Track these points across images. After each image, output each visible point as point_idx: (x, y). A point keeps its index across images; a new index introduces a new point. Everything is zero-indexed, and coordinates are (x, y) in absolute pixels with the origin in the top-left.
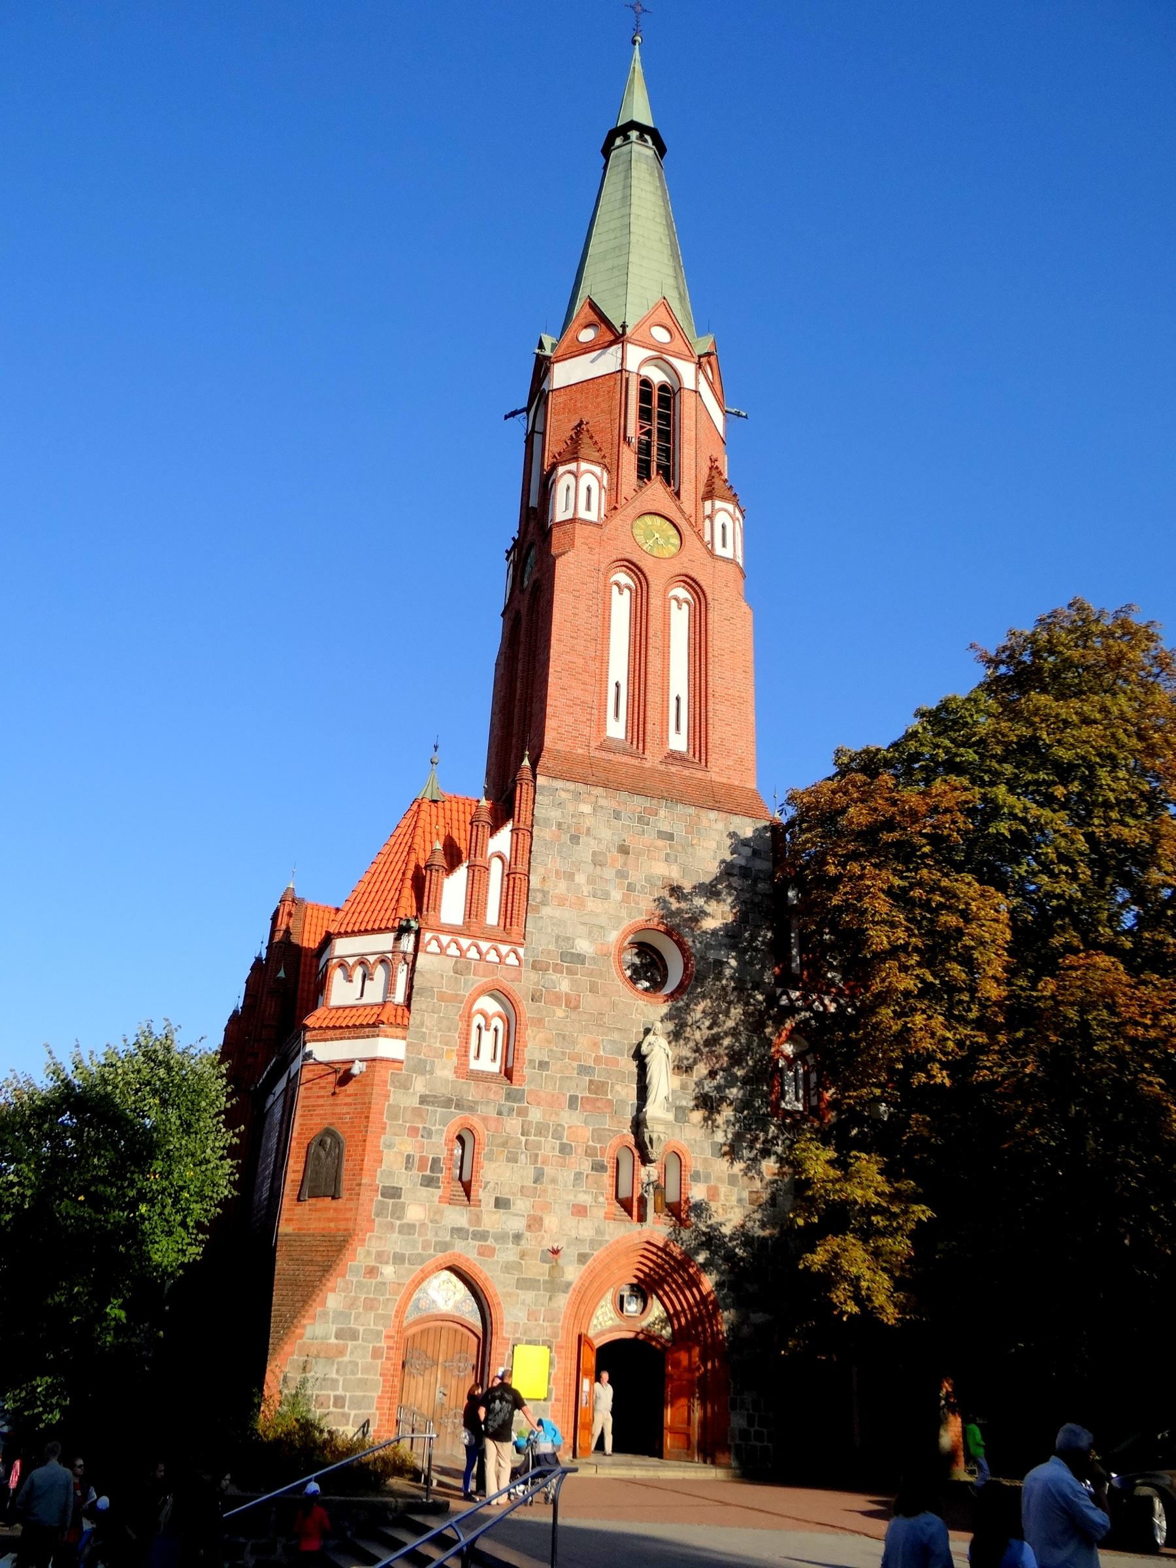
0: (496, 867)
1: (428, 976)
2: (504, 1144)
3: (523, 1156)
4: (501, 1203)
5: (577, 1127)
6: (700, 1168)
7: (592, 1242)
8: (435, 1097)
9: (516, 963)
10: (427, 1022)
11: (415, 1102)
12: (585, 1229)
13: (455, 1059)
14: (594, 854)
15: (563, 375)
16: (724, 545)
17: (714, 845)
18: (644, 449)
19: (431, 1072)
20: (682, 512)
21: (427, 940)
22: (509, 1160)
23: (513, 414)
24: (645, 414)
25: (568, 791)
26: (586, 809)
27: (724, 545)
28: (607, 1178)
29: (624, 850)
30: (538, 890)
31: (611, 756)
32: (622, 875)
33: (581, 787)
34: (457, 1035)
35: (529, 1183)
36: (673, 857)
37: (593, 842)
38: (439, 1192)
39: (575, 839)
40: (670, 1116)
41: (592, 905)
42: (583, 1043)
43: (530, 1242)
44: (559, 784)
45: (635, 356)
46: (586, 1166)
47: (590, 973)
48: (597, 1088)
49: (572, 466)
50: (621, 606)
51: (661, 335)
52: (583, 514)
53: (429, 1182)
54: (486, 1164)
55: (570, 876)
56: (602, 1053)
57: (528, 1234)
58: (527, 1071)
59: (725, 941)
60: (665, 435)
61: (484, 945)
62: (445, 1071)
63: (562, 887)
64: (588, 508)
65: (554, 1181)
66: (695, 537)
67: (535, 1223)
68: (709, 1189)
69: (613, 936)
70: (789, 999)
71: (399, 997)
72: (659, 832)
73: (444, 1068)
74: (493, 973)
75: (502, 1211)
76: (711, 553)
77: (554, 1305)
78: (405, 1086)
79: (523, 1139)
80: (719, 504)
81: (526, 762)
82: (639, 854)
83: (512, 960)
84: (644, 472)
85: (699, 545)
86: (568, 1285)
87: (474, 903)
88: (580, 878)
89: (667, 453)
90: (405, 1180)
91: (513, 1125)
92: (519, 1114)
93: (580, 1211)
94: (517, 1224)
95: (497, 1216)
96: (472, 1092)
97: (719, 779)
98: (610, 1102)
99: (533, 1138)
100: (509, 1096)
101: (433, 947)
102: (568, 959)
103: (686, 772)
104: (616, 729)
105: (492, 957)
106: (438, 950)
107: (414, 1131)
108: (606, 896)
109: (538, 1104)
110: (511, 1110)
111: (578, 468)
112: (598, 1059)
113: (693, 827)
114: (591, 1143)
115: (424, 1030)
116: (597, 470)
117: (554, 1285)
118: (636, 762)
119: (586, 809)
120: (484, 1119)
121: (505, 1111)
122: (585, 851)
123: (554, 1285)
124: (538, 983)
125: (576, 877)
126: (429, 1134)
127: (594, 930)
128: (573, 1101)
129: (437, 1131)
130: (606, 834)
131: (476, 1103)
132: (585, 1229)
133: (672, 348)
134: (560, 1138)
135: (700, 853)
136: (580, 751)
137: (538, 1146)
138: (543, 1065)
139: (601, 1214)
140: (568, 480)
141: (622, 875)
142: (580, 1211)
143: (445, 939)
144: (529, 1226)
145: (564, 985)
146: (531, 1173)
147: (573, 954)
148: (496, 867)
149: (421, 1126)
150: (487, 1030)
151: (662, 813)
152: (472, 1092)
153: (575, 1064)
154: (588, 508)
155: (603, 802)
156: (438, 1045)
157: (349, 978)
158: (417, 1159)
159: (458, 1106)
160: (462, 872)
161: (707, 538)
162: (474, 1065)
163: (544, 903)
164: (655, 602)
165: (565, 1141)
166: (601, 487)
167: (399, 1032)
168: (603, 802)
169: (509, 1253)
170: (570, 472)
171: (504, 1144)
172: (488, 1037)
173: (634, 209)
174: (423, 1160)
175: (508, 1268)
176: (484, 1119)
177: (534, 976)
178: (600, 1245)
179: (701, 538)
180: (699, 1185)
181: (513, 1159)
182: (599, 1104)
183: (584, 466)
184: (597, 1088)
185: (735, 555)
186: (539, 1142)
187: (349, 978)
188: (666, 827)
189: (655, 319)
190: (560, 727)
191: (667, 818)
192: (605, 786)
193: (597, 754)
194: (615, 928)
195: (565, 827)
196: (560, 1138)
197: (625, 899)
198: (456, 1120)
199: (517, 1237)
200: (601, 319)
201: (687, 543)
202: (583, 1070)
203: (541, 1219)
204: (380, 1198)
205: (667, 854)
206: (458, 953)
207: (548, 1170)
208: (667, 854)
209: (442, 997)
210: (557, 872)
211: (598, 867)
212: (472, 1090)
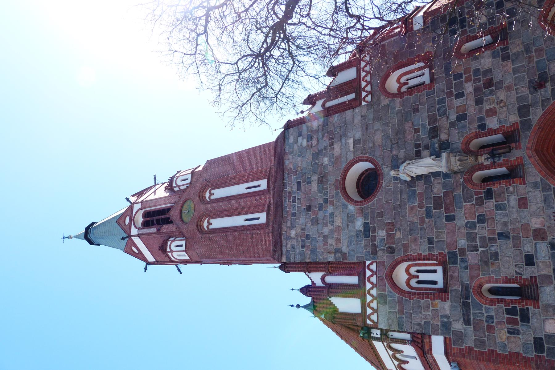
0: (330, 279)
1: (390, 321)
3: (492, 248)
4: (530, 260)
5: (465, 213)
6: (476, 125)
7: (544, 190)
8: (463, 314)
9: (375, 264)
10: (418, 321)
11: (470, 329)
13: (437, 301)
14: (313, 225)
17: (299, 159)
19: (448, 317)
20: (178, 201)
21: (371, 323)
22: (497, 259)
23: (179, 270)
25: (287, 244)
26: (293, 233)
28: (496, 188)
30: (335, 255)
32: (321, 208)
33: (284, 235)
34: (422, 301)
35: (510, 243)
36: (308, 180)
38: (531, 308)
39: (308, 237)
40: (444, 155)
41: (338, 223)
42: (413, 218)
44: (284, 249)
46: (490, 204)
47: (373, 218)
50: (218, 223)
52: (183, 248)
53: (525, 318)
55: (326, 237)
56: (416, 204)
58: (436, 252)
59: (343, 141)
62: (445, 307)
63: (331, 242)
65: (505, 224)
67: (539, 235)
68: (488, 116)
69: (351, 208)
72: (298, 190)
73: (444, 309)
74: (382, 279)
75: (535, 260)
76: (190, 184)
78: (460, 336)
79: (480, 249)
80: (174, 185)
82: (309, 199)
84: (168, 221)
85: (188, 192)
88: (326, 231)
90: (527, 336)
91: (472, 258)
92: (465, 255)
93: (523, 203)
95: (540, 264)
97: (273, 162)
98: (446, 194)
99: (478, 243)
100: (455, 263)
102: (367, 233)
106: (375, 315)
107: (490, 328)
108: (332, 215)
109: (455, 242)
111: (169, 252)
112: (421, 206)
114: (474, 202)
115: (423, 323)
116: (169, 243)
122: (312, 230)
124: (383, 251)
125: (325, 234)
126: (490, 317)
127: (351, 219)
128: (450, 218)
129: (487, 312)
131: (463, 285)
132: (536, 197)
134: (473, 226)
136: (271, 238)
137: (483, 239)
138: (430, 241)
139: (521, 187)
142: (523, 203)
143: (369, 311)
144: (543, 239)
145: (382, 233)
147: (364, 230)
148: (330, 279)
149: (486, 324)
150: (418, 277)
151: (289, 190)
153: (426, 220)
155: (289, 224)
156: (430, 313)
158: (510, 326)
159: (467, 298)
162: (440, 285)
164: (210, 207)
165: (476, 220)
166: (175, 240)
167: (426, 340)
172: (423, 277)
174: (509, 321)
176: (472, 278)
177: (380, 253)
178: (546, 184)
180: (487, 123)
181: (496, 255)
182: (448, 201)
183: (168, 250)
184: (437, 203)
186: (480, 238)
188: (295, 187)
189: (123, 224)
191: (292, 188)
193: (271, 228)
194: (347, 207)
197: (332, 203)
202: (429, 214)
203: (535, 230)
204: (545, 354)
207: (499, 229)
208: (308, 183)
210: (324, 245)
211: (319, 222)
212: (455, 288)
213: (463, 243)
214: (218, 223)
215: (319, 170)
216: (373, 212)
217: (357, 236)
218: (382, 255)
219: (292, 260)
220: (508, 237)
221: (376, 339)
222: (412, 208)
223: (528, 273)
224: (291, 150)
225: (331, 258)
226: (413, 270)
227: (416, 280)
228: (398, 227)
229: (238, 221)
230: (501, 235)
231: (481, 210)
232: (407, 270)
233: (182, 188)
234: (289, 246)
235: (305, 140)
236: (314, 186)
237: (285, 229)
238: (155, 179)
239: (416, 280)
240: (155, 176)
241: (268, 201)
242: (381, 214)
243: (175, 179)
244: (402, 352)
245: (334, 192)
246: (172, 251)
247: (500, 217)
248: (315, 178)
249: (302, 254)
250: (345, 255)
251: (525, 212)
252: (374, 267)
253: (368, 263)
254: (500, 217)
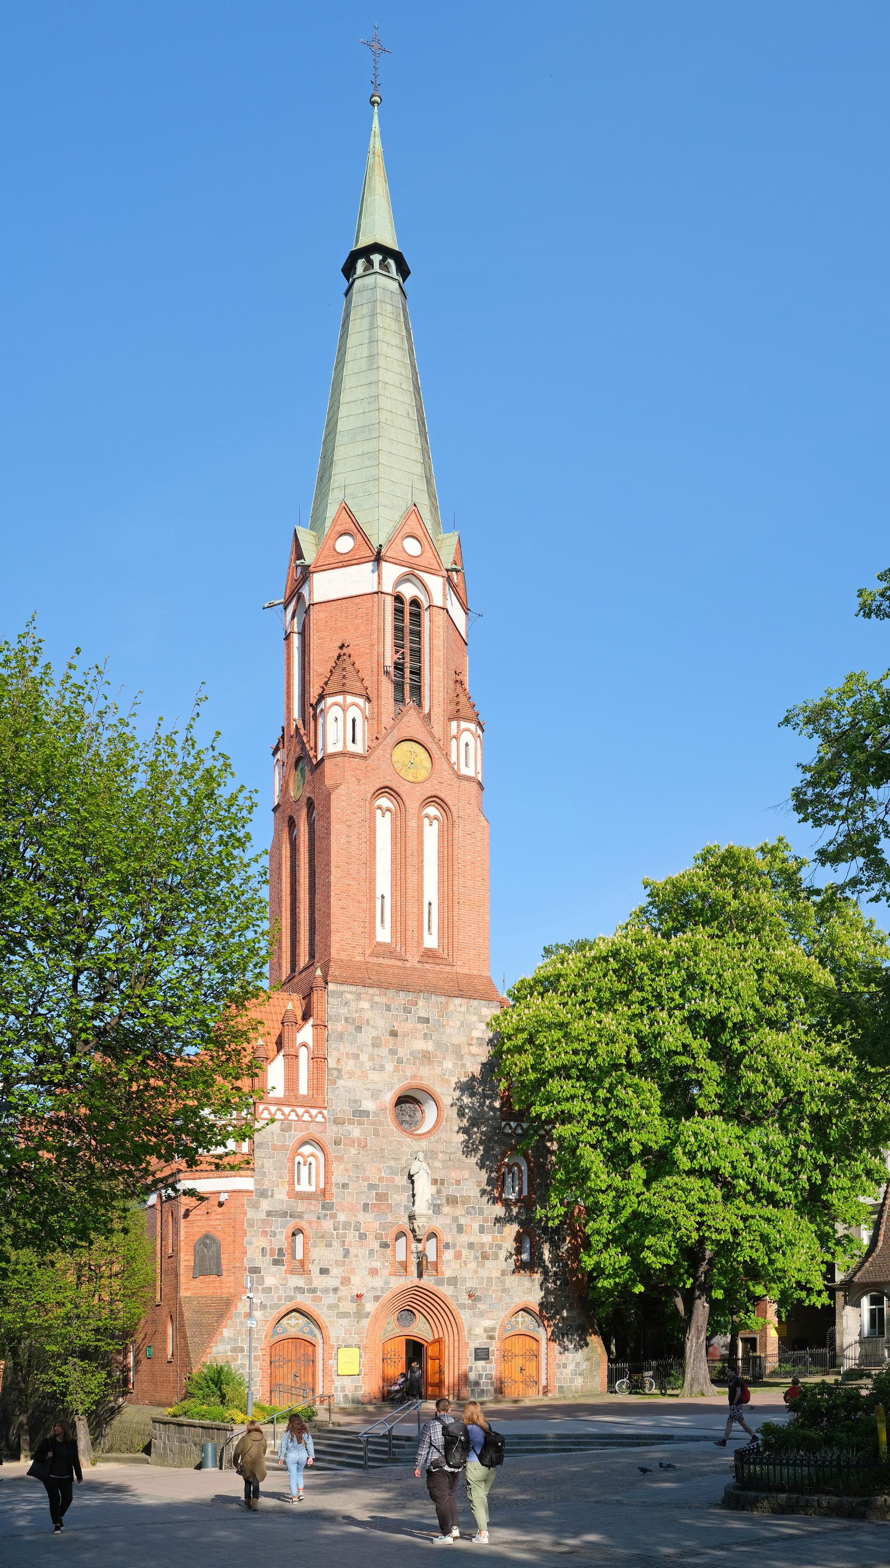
2: (322, 1237)
4: (324, 1271)
12: (378, 1282)
15: (325, 586)
17: (458, 1023)
22: (326, 1246)
25: (351, 993)
26: (365, 1005)
29: (394, 1034)
31: (381, 960)
32: (393, 1052)
33: (360, 989)
35: (341, 1258)
37: (371, 1030)
39: (359, 1029)
43: (343, 1291)
45: (391, 572)
46: (376, 1245)
48: (382, 1197)
50: (384, 826)
51: (412, 547)
54: (312, 1249)
55: (356, 1057)
57: (342, 1288)
58: (334, 1190)
60: (417, 654)
61: (301, 1111)
63: (350, 1065)
65: (356, 1256)
66: (444, 760)
67: (346, 1281)
69: (389, 1097)
70: (522, 1129)
77: (360, 1325)
81: (319, 972)
82: (405, 1035)
83: (320, 1119)
84: (399, 699)
86: (369, 1314)
87: (291, 1081)
88: (364, 1058)
93: (373, 1272)
94: (336, 1283)
96: (301, 1206)
100: (323, 1207)
103: (438, 968)
104: (383, 935)
105: (306, 1117)
108: (382, 1068)
110: (326, 1215)
112: (381, 1179)
113: (443, 1011)
117: (360, 1315)
118: (399, 963)
119: (365, 1005)
120: (309, 1222)
121: (321, 1216)
122: (367, 1035)
123: (360, 1315)
127: (375, 1095)
128: (366, 1207)
130: (380, 1023)
133: (421, 562)
134: (358, 1230)
135: (448, 1030)
136: (358, 958)
137: (345, 1236)
138: (345, 1186)
141: (393, 1052)
142: (373, 1272)
146: (341, 1252)
148: (303, 1053)
151: (421, 1003)
152: (301, 1206)
153: (366, 1184)
155: (377, 999)
160: (280, 1060)
162: (298, 1188)
163: (340, 1077)
164: (412, 824)
168: (377, 999)
169: (331, 1299)
171: (322, 1237)
173: (383, 375)
175: (331, 1307)
176: (309, 1222)
177: (335, 1128)
179: (449, 761)
181: (329, 1245)
184: (382, 1197)
185: (477, 773)
188: (423, 1014)
190: (342, 943)
191: (424, 1007)
192: (379, 987)
193: (371, 960)
195: (350, 1020)
196: (358, 1230)
197: (396, 1069)
198: (292, 1224)
199: (335, 1290)
200: (357, 531)
201: (436, 761)
202: (371, 1187)
205: (425, 1034)
206: (282, 1117)
208: (425, 1034)
209: (274, 1148)
213: (342, 1217)
214: (384, 826)
215: (438, 1054)
216: (381, 1123)
217: (356, 1101)
218: (333, 1131)
219: (331, 1000)
220: (345, 1256)
222: (379, 1170)
223: (314, 1269)
224: (471, 1009)
225: (332, 1063)
226: (311, 1159)
227: (302, 1162)
228: (362, 1152)
229: (383, 884)
230: (347, 1253)
231: (371, 1237)
232: (312, 1155)
234: (349, 996)
235: (480, 1035)
236: (420, 1045)
237: (371, 991)
239: (302, 1162)
241: (408, 957)
242: (376, 1134)
245: (408, 1073)
247: (363, 1252)
248: (429, 1046)
249: (337, 1018)
250: (335, 1083)
251: (365, 1273)
252: (320, 1119)
253: (325, 1112)
254: (363, 1252)
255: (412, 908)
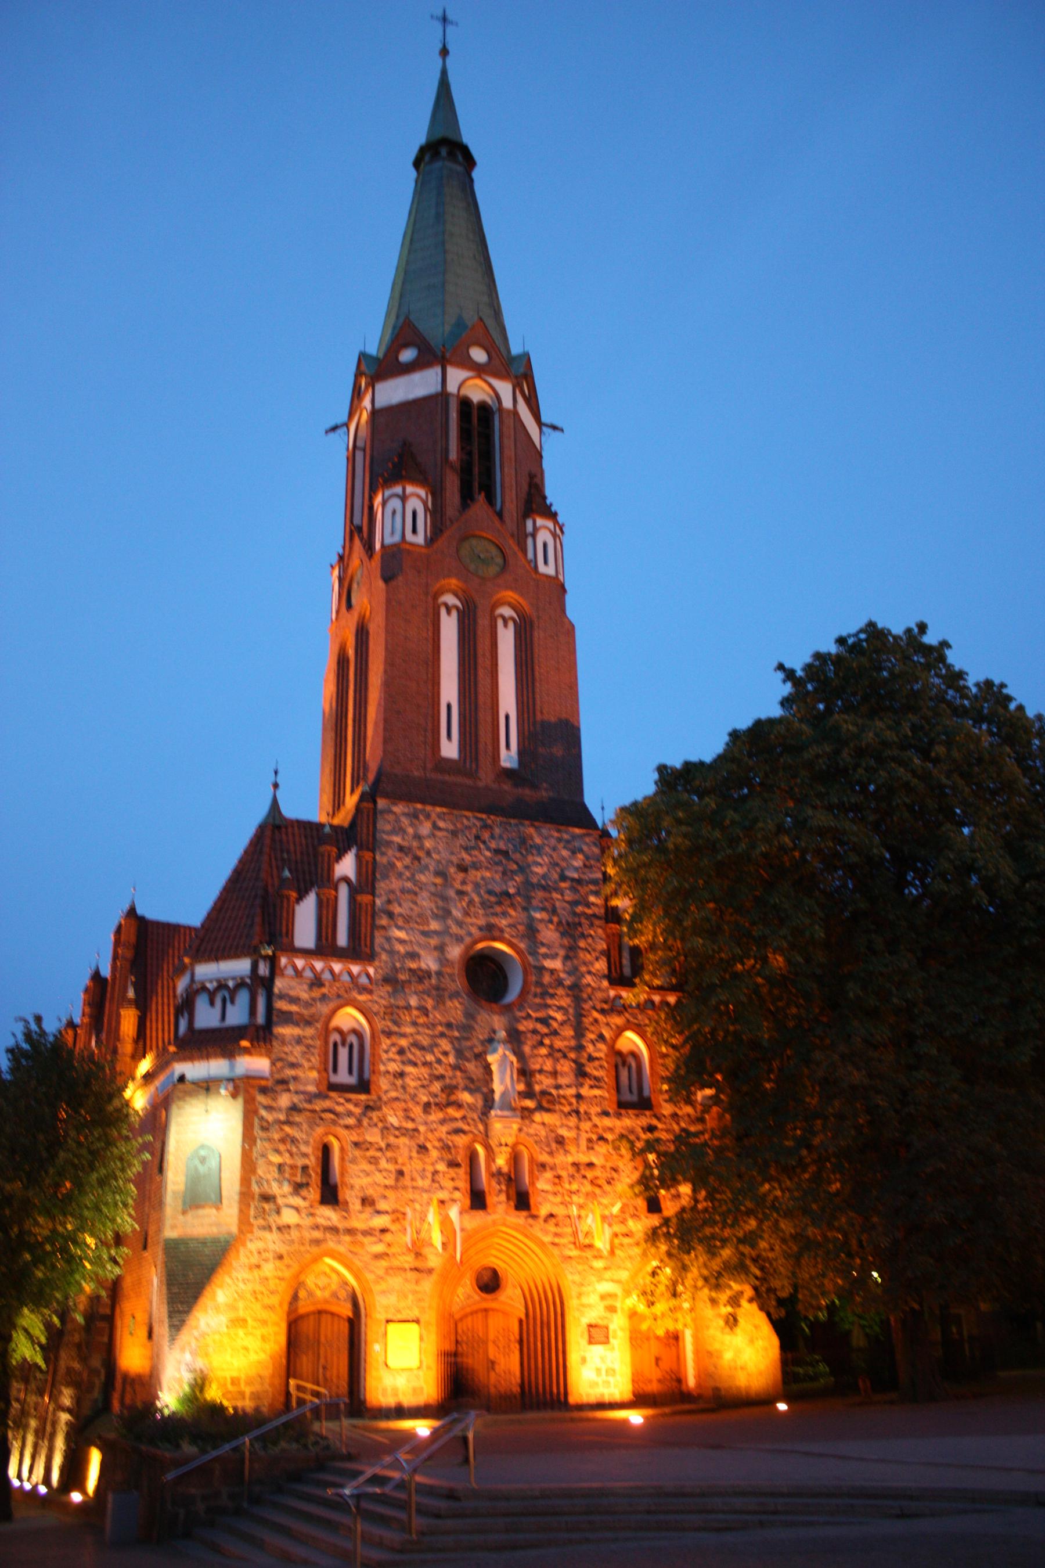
0: (343, 891)
16: (546, 562)
18: (465, 471)
24: (465, 434)
26: (425, 829)
27: (546, 562)
49: (398, 490)
50: (449, 628)
60: (487, 455)
64: (414, 531)
71: (260, 1019)
80: (540, 522)
89: (488, 473)
101: (290, 971)
116: (422, 492)
119: (425, 829)
140: (395, 503)
143: (300, 963)
150: (343, 1044)
154: (414, 531)
157: (212, 1003)
161: (530, 555)
164: (483, 622)
170: (397, 495)
183: (410, 489)
187: (212, 1003)
221: (255, 967)
233: (530, 541)
238: (554, 428)
240: (562, 430)
243: (550, 524)
244: (232, 1002)
246: (404, 498)
255: (484, 716)
